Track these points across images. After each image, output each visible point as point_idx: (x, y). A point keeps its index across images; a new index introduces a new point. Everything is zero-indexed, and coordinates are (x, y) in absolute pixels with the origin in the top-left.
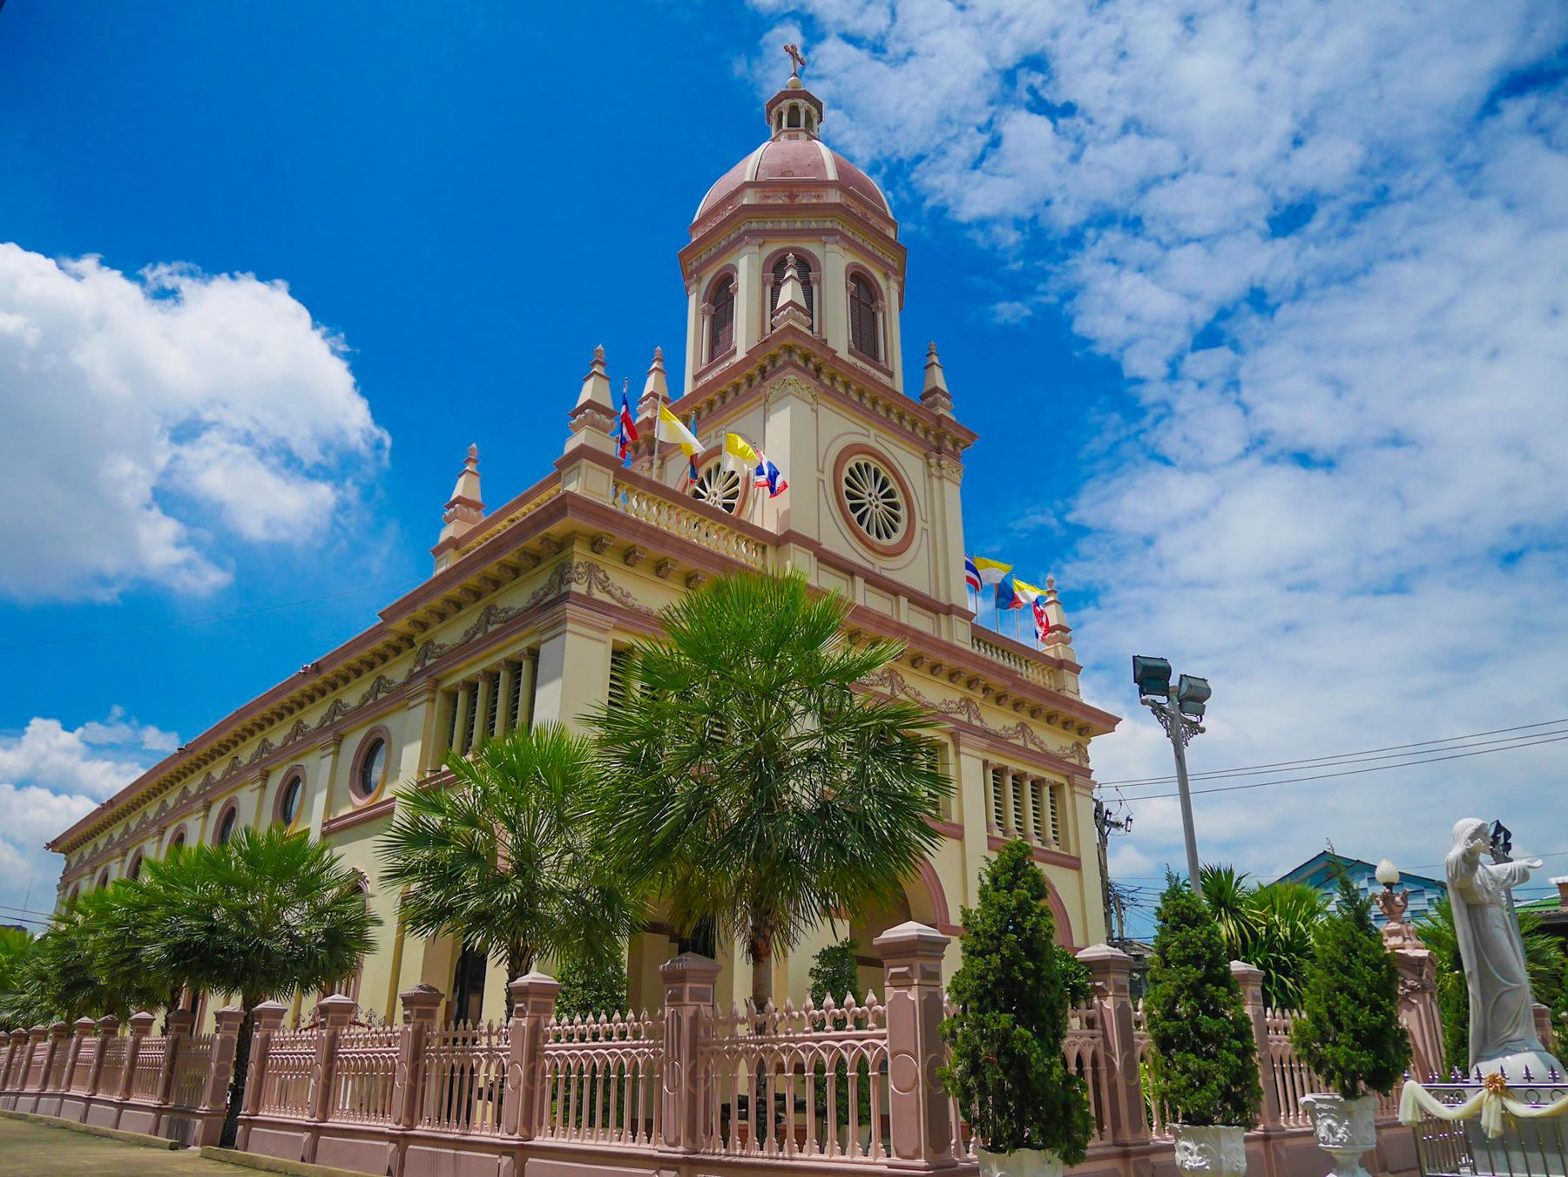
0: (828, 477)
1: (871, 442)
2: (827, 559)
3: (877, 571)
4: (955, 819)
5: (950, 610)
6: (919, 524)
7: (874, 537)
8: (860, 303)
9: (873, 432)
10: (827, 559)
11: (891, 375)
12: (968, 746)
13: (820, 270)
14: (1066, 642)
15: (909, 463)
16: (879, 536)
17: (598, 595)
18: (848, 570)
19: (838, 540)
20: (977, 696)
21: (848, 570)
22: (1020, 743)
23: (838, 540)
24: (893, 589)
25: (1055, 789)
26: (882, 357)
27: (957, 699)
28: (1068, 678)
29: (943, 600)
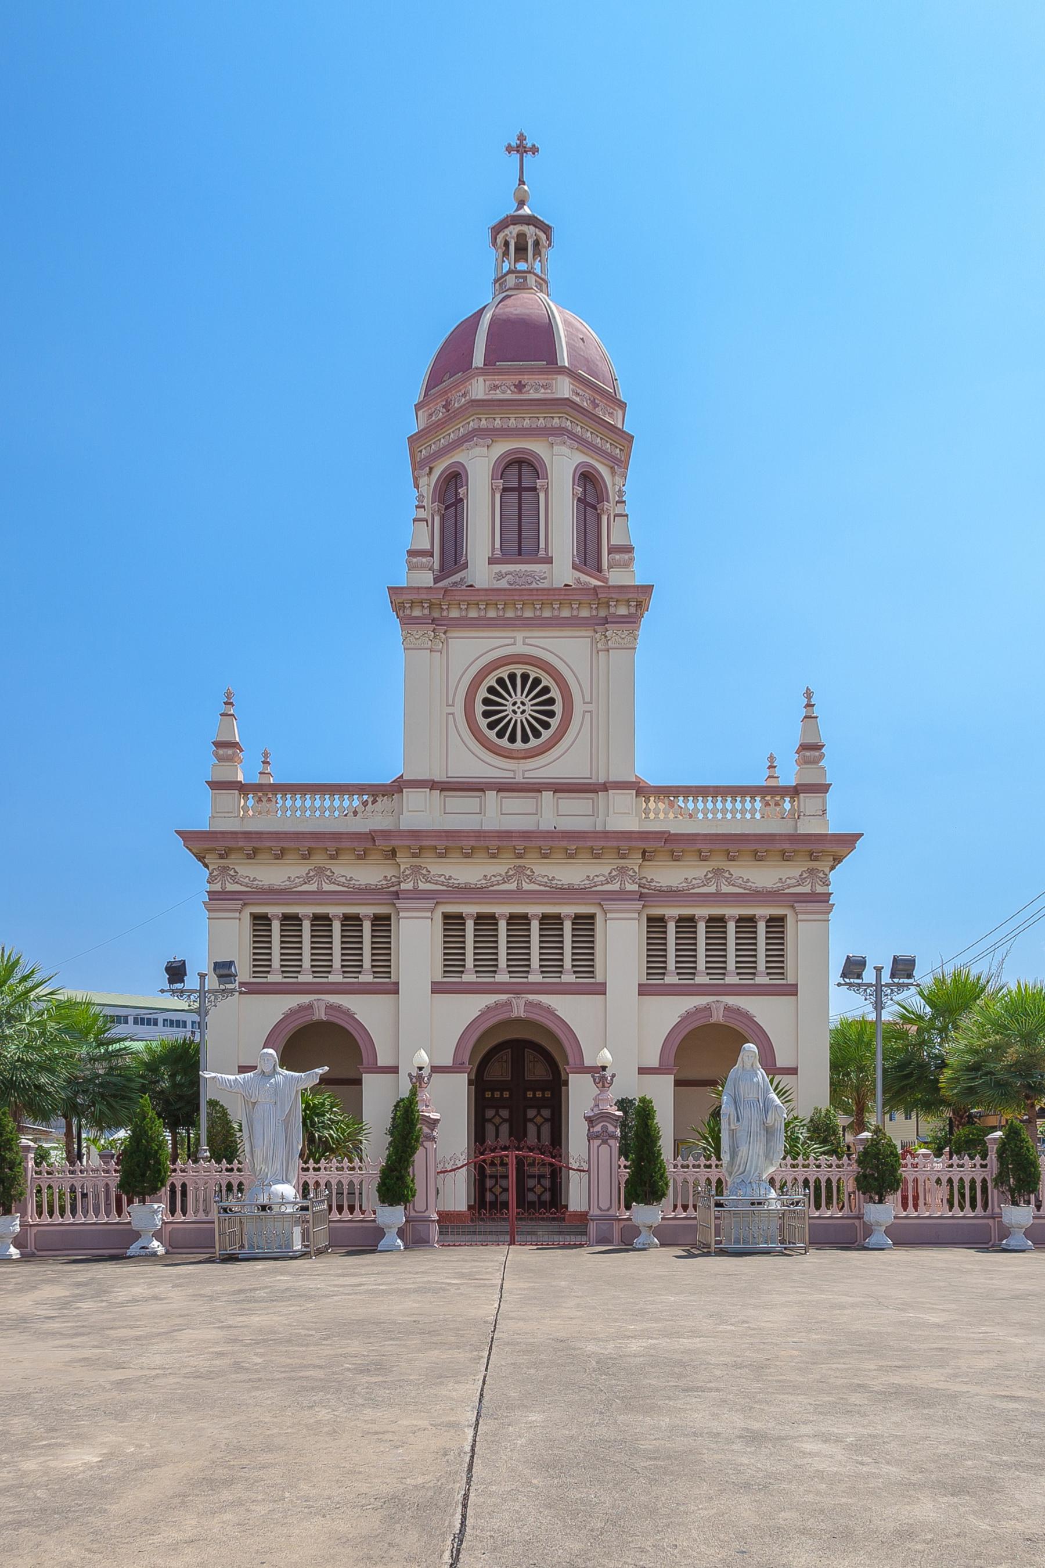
0: (459, 709)
1: (519, 649)
2: (446, 787)
3: (519, 779)
4: (599, 979)
5: (605, 787)
6: (578, 707)
7: (519, 744)
8: (520, 489)
9: (520, 636)
10: (446, 787)
11: (549, 561)
12: (611, 911)
13: (467, 485)
14: (816, 761)
15: (566, 651)
16: (525, 739)
17: (231, 887)
18: (477, 788)
19: (472, 761)
20: (634, 862)
21: (477, 788)
22: (712, 889)
23: (472, 761)
24: (535, 788)
25: (776, 923)
26: (542, 545)
27: (605, 870)
28: (808, 802)
29: (601, 781)
